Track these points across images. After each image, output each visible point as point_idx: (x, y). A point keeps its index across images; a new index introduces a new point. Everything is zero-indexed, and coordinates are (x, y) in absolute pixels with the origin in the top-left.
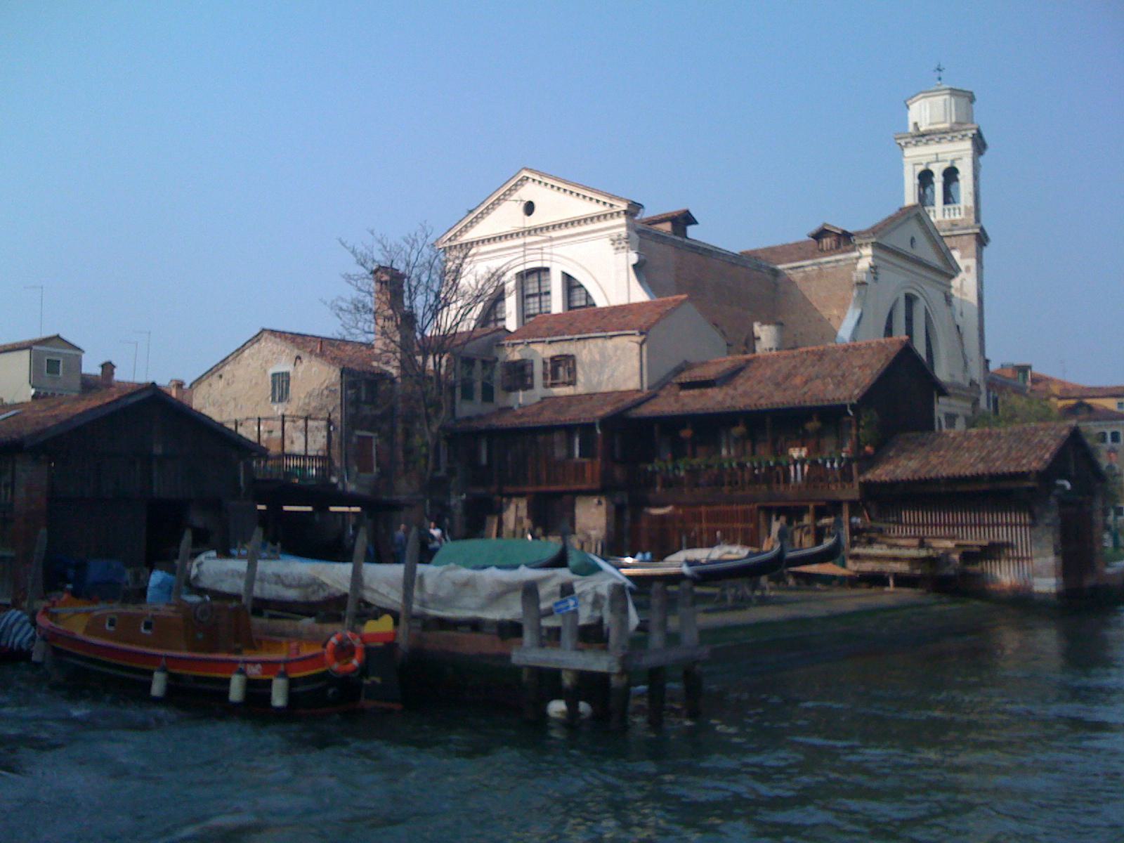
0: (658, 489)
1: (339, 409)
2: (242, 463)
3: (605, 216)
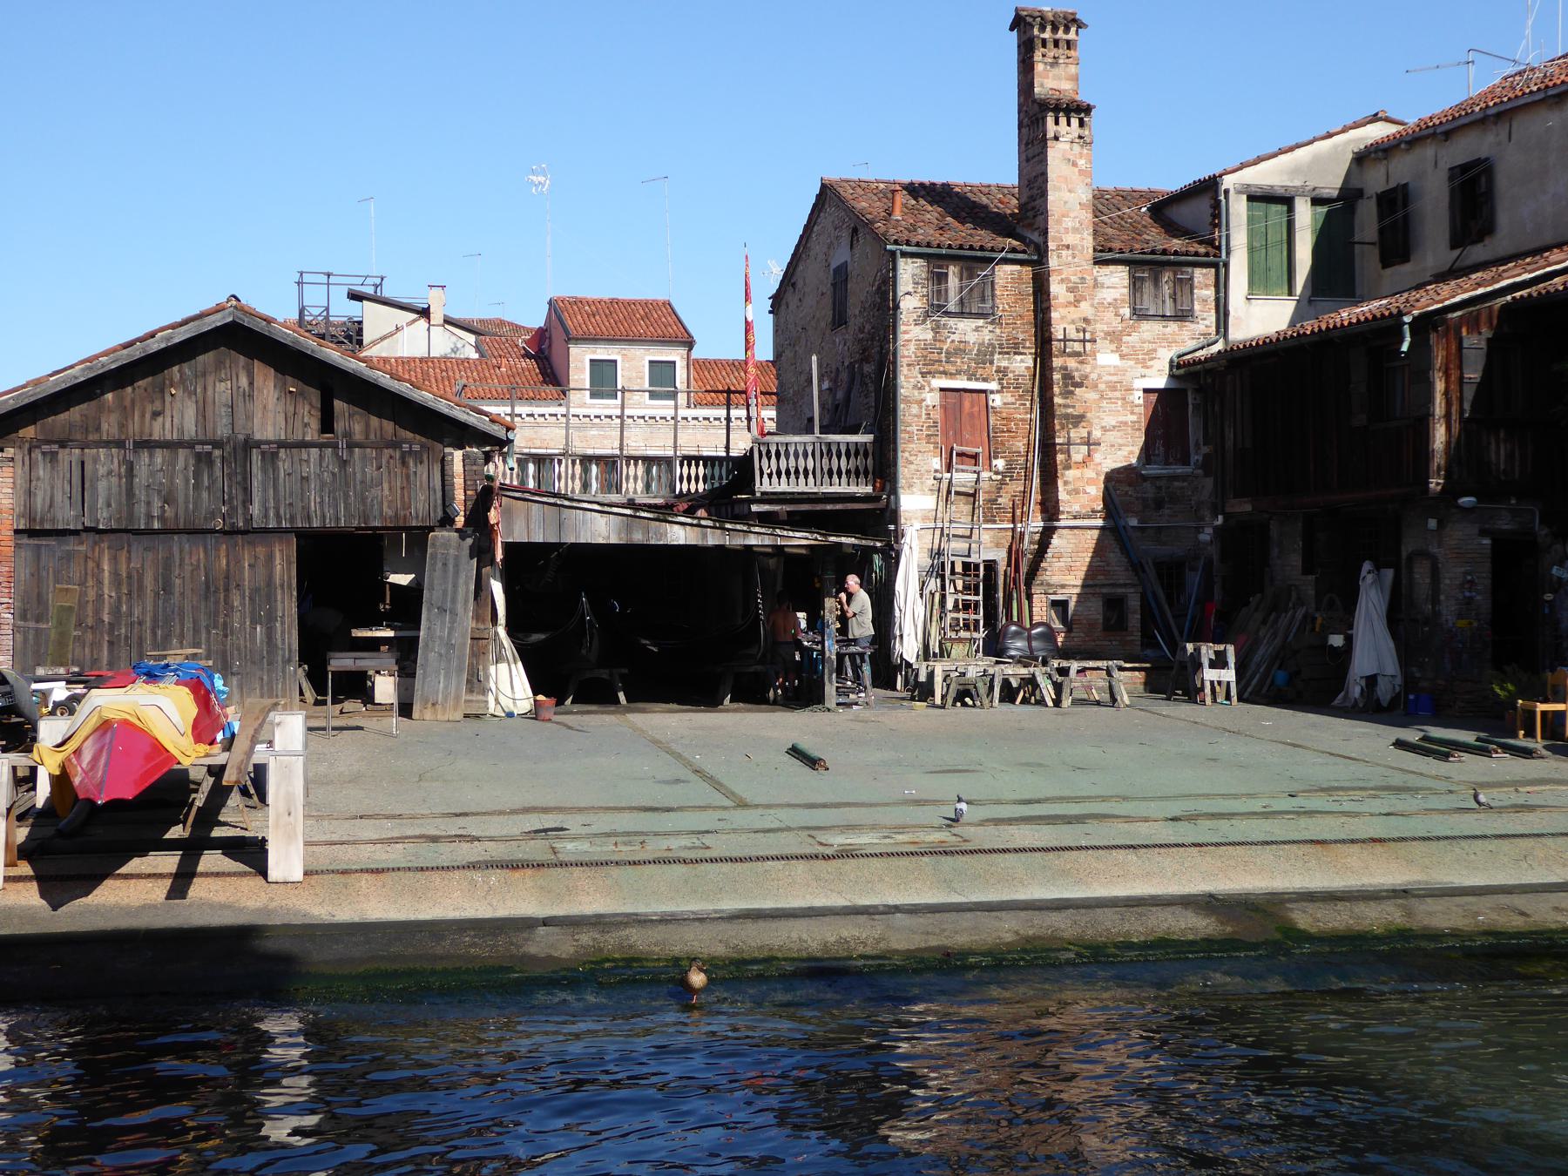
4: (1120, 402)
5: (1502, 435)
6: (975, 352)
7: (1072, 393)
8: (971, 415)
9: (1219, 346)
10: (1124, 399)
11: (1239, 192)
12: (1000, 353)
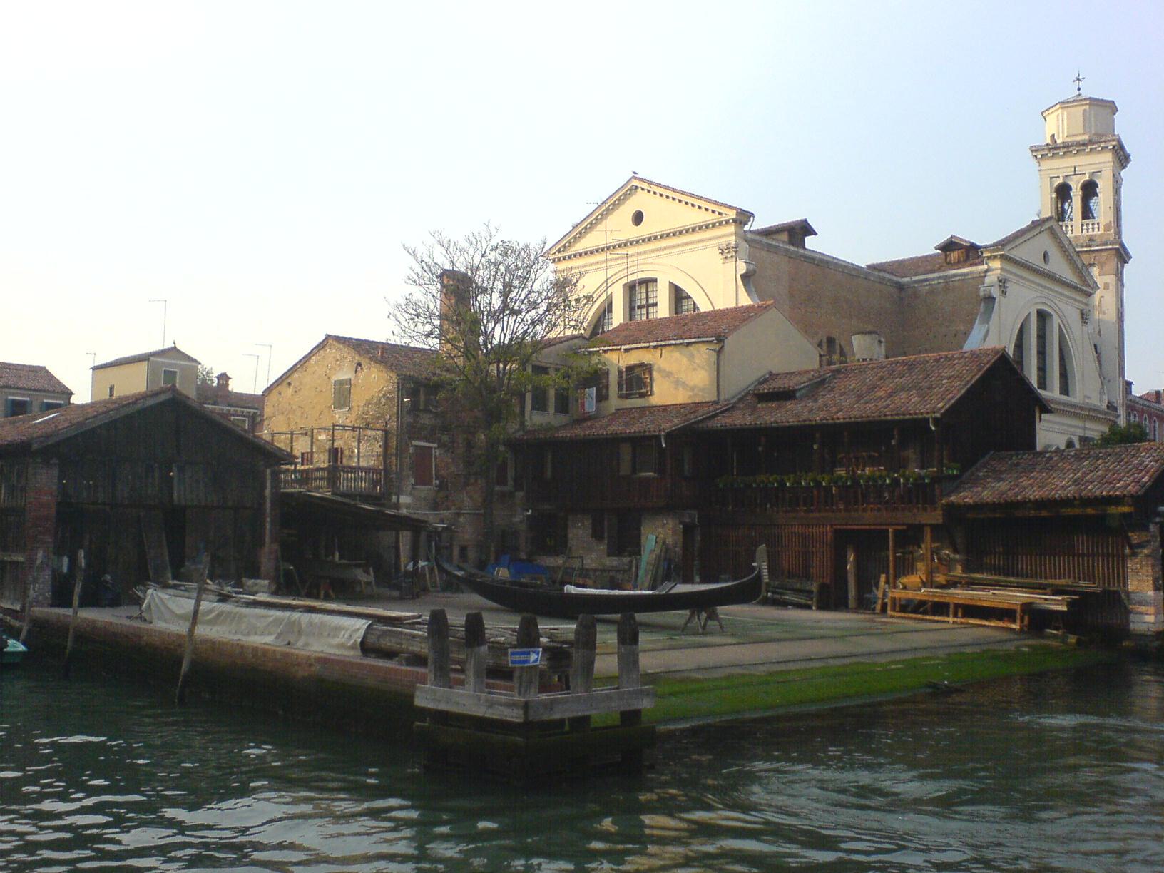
0: (730, 507)
1: (394, 418)
2: (268, 471)
3: (714, 225)
9: (521, 433)
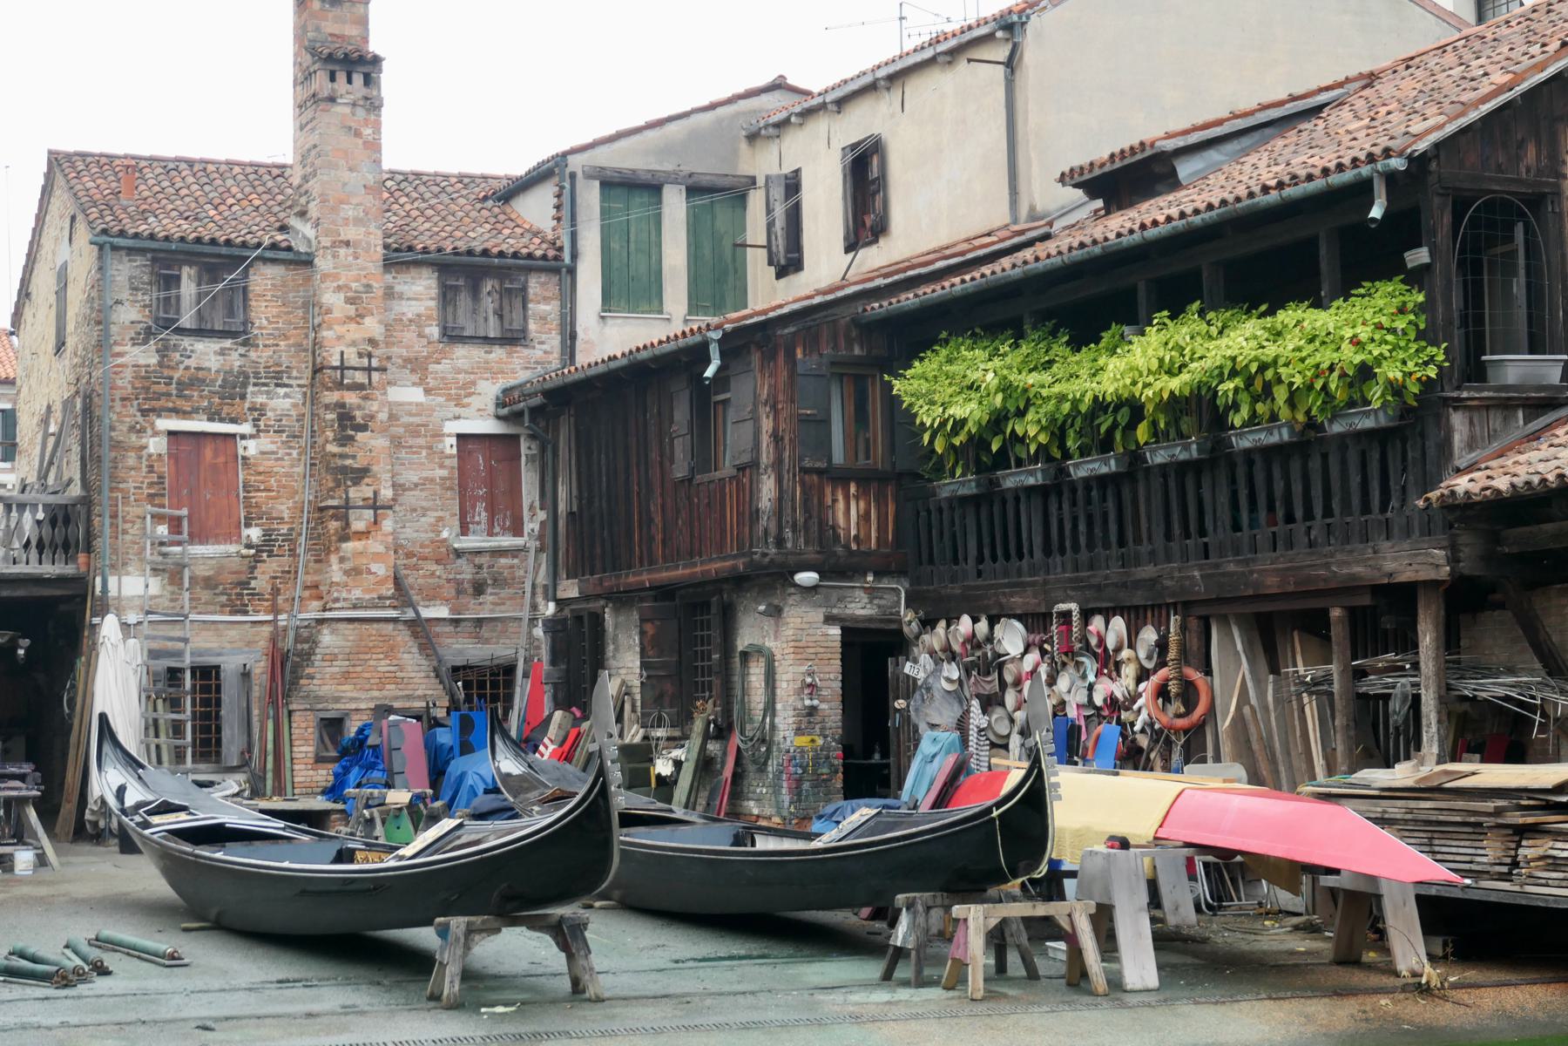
4: (424, 453)
5: (853, 490)
6: (219, 382)
7: (352, 438)
8: (214, 467)
10: (430, 448)
11: (589, 176)
12: (255, 385)
